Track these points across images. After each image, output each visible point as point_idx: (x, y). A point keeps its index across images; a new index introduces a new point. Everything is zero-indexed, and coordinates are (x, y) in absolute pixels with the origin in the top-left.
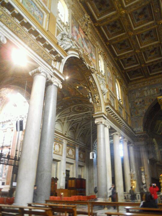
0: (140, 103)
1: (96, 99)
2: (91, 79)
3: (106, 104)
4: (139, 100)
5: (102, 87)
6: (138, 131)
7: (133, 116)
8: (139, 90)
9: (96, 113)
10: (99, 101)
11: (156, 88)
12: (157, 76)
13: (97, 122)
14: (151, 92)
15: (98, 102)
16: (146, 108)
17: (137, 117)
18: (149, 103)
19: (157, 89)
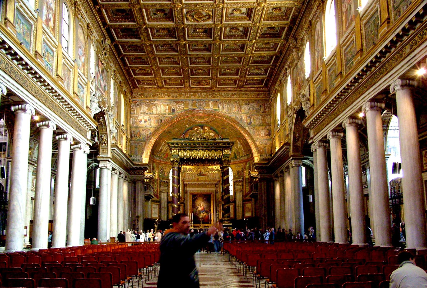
0: (145, 121)
1: (103, 139)
2: (102, 119)
3: (113, 145)
4: (145, 118)
5: (111, 125)
7: (134, 138)
8: (147, 103)
9: (101, 156)
10: (105, 143)
11: (168, 105)
12: (173, 90)
13: (102, 166)
14: (162, 109)
15: (104, 143)
17: (138, 141)
18: (157, 125)
19: (169, 107)
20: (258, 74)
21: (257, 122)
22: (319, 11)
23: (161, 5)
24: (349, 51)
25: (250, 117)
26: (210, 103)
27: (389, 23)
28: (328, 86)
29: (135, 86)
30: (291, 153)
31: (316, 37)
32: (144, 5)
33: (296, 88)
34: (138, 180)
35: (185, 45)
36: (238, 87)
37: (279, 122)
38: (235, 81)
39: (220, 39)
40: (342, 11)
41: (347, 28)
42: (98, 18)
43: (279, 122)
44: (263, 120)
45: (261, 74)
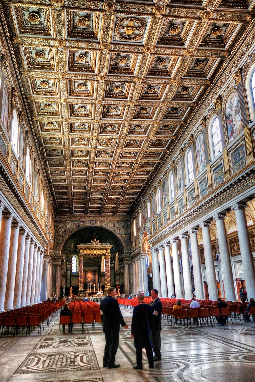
0: (62, 232)
6: (57, 254)
7: (56, 241)
16: (66, 237)
20: (124, 209)
21: (123, 232)
22: (153, 192)
23: (81, 185)
24: (165, 216)
25: (119, 230)
26: (98, 222)
27: (177, 214)
28: (158, 227)
29: (57, 213)
30: (142, 252)
31: (153, 202)
32: (73, 185)
33: (144, 220)
34: (58, 265)
35: (89, 198)
36: (113, 214)
37: (135, 234)
38: (112, 212)
39: (107, 196)
40: (163, 198)
41: (165, 206)
42: (49, 188)
43: (135, 234)
44: (126, 232)
45: (125, 209)
